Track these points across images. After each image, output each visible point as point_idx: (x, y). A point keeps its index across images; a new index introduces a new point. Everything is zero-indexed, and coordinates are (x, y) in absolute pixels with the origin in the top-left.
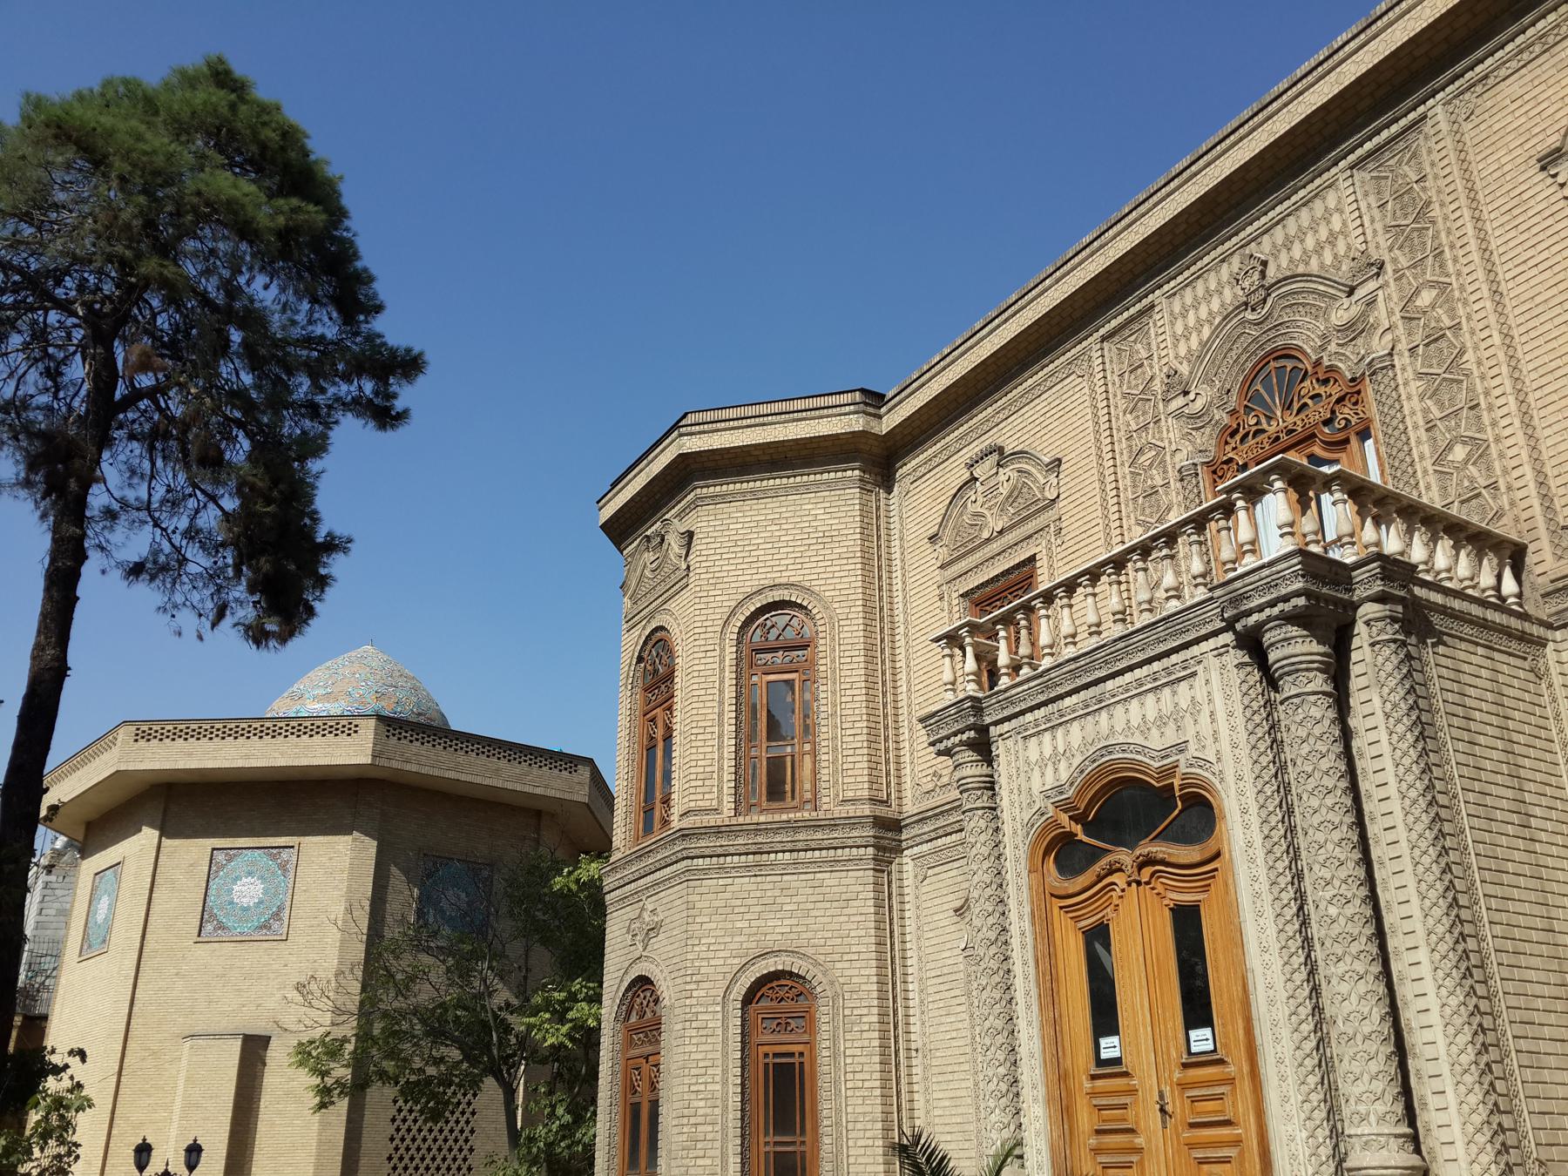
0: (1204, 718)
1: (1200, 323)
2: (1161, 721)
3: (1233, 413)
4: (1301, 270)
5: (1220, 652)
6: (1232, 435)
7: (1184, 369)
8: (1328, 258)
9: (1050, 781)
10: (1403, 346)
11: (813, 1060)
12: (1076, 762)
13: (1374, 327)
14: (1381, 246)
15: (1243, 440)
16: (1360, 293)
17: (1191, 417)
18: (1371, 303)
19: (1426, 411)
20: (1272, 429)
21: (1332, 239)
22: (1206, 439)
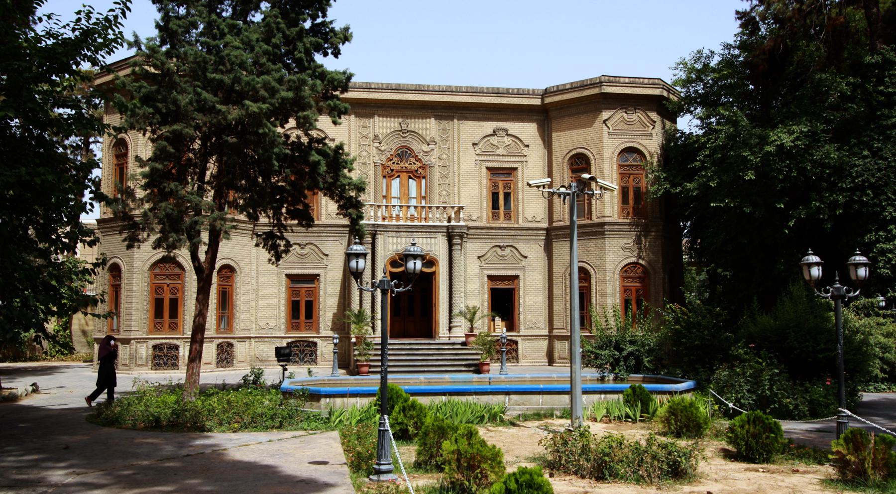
0: (437, 247)
1: (387, 128)
2: (427, 244)
3: (392, 155)
4: (417, 131)
5: (442, 236)
6: (391, 160)
7: (380, 136)
8: (417, 126)
9: (395, 248)
10: (437, 163)
11: (232, 290)
12: (403, 246)
13: (432, 155)
14: (438, 139)
15: (394, 163)
16: (431, 146)
17: (380, 150)
18: (432, 150)
19: (439, 180)
20: (402, 164)
21: (426, 129)
22: (384, 158)
